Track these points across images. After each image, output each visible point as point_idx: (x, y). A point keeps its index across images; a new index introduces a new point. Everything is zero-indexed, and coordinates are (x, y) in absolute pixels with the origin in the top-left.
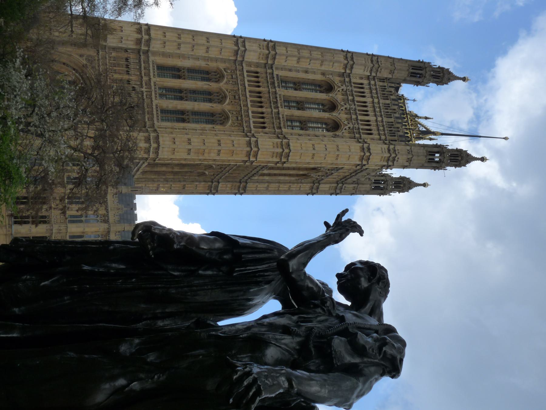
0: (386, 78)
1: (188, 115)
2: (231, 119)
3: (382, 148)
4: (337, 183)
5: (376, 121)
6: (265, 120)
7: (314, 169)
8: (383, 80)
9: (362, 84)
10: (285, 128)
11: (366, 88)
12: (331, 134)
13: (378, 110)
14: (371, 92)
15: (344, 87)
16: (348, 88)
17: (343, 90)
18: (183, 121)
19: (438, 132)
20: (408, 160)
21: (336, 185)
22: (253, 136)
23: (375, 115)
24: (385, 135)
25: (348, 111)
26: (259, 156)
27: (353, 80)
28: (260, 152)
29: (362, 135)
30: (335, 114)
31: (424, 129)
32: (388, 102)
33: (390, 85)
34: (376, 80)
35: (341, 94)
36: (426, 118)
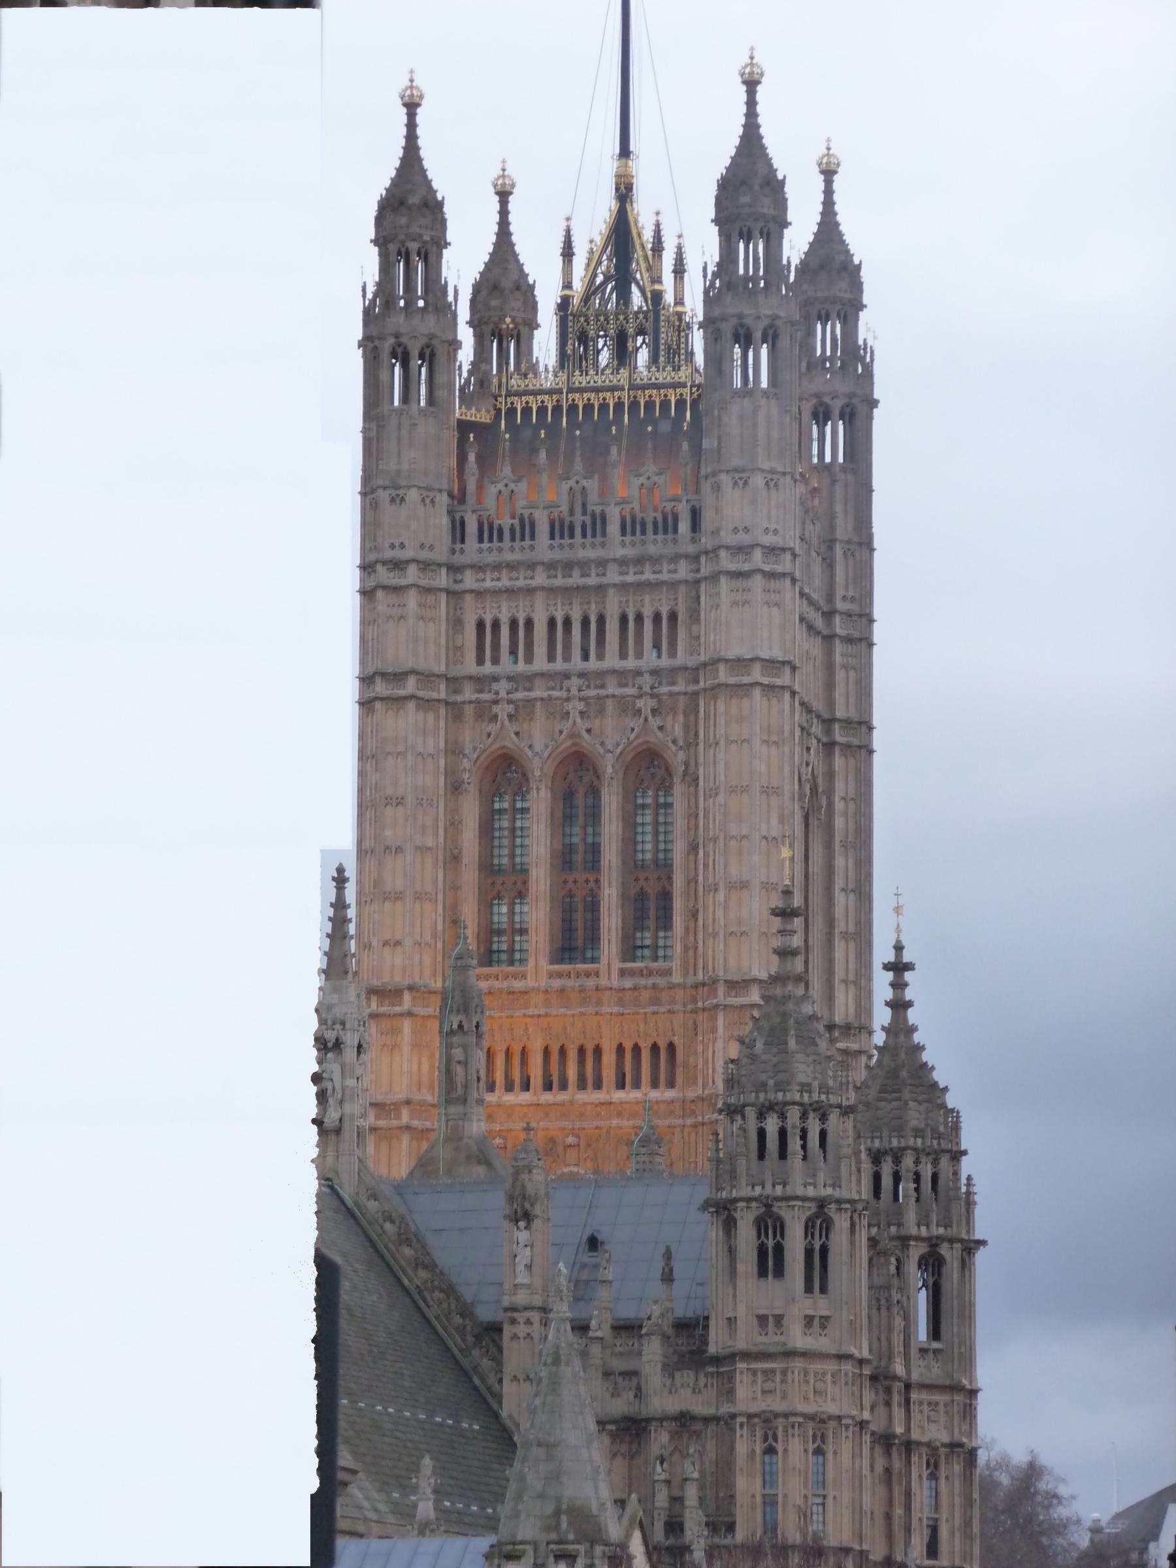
0: (450, 512)
3: (735, 603)
4: (829, 638)
8: (458, 530)
9: (480, 625)
10: (668, 972)
11: (495, 611)
12: (678, 789)
13: (576, 579)
14: (510, 592)
15: (503, 710)
16: (503, 694)
17: (510, 716)
19: (618, 176)
20: (772, 484)
27: (470, 666)
29: (682, 658)
30: (609, 766)
32: (543, 529)
33: (471, 498)
34: (459, 559)
35: (526, 726)
36: (568, 253)
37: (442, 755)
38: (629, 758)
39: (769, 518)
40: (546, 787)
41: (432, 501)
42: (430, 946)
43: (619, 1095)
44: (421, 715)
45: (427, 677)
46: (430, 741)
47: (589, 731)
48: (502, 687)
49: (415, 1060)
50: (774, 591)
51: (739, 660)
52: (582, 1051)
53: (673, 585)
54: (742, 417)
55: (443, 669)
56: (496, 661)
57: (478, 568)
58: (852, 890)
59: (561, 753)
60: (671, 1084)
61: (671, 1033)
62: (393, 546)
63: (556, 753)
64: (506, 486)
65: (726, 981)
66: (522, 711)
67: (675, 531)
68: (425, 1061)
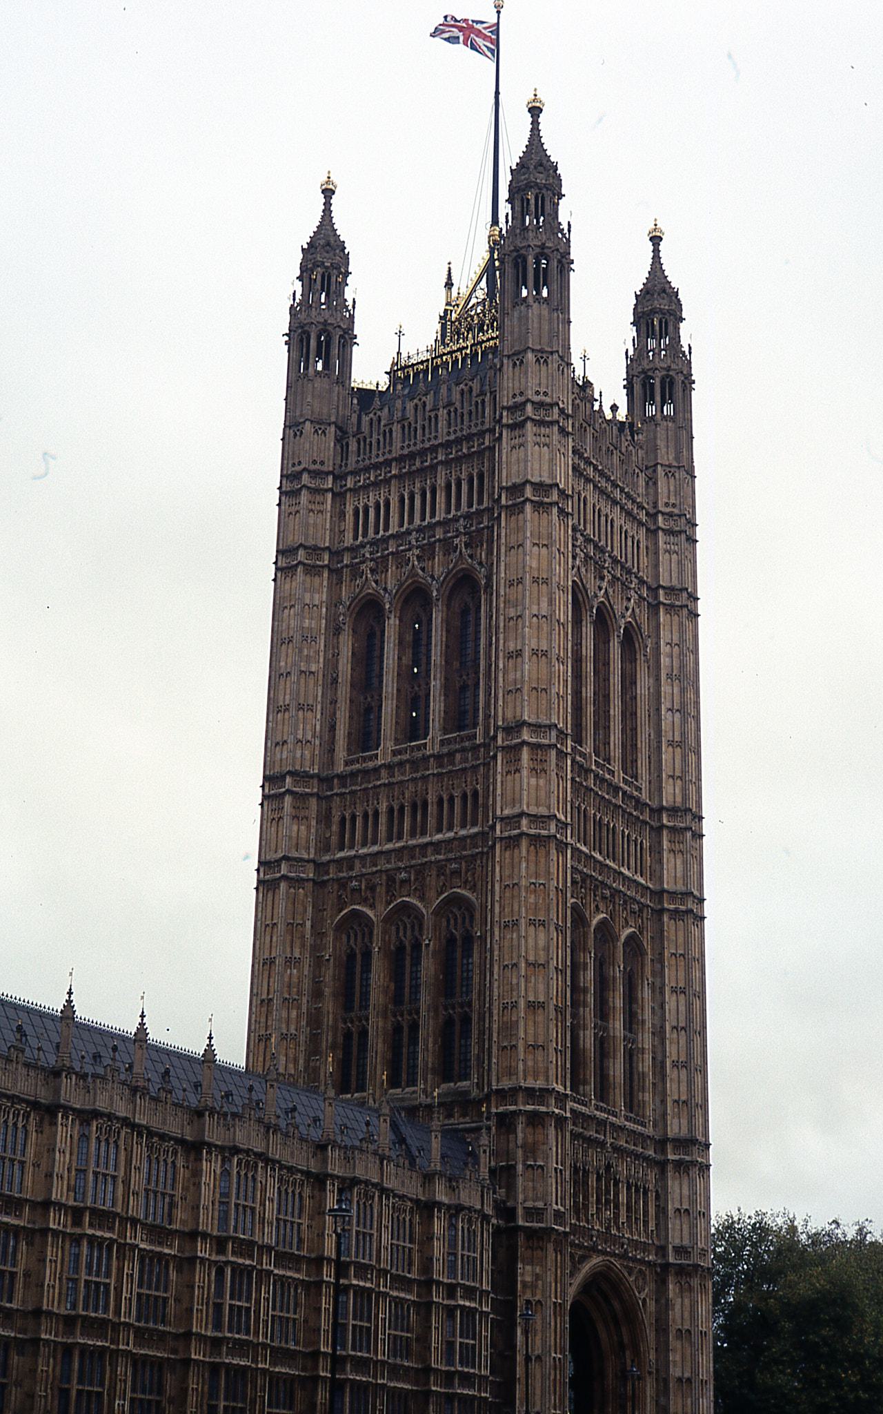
0: (338, 440)
1: (453, 1008)
2: (459, 891)
4: (653, 533)
5: (447, 463)
6: (457, 793)
7: (603, 621)
14: (376, 484)
16: (368, 555)
17: (372, 571)
18: (466, 1020)
21: (660, 533)
22: (493, 827)
23: (433, 468)
24: (481, 434)
25: (427, 552)
26: (543, 811)
27: (349, 540)
28: (533, 810)
31: (483, 284)
36: (449, 284)
37: (324, 604)
38: (450, 584)
39: (540, 384)
40: (395, 617)
41: (324, 432)
42: (311, 743)
43: (439, 837)
44: (308, 579)
45: (315, 550)
46: (317, 596)
47: (423, 569)
48: (367, 552)
49: (295, 828)
50: (544, 436)
51: (515, 486)
52: (414, 807)
53: (480, 453)
54: (520, 318)
55: (327, 545)
56: (365, 534)
57: (355, 473)
58: (677, 710)
59: (404, 591)
60: (474, 824)
61: (474, 782)
62: (294, 465)
63: (401, 590)
64: (375, 414)
65: (504, 729)
66: (380, 566)
67: (483, 417)
68: (303, 828)
